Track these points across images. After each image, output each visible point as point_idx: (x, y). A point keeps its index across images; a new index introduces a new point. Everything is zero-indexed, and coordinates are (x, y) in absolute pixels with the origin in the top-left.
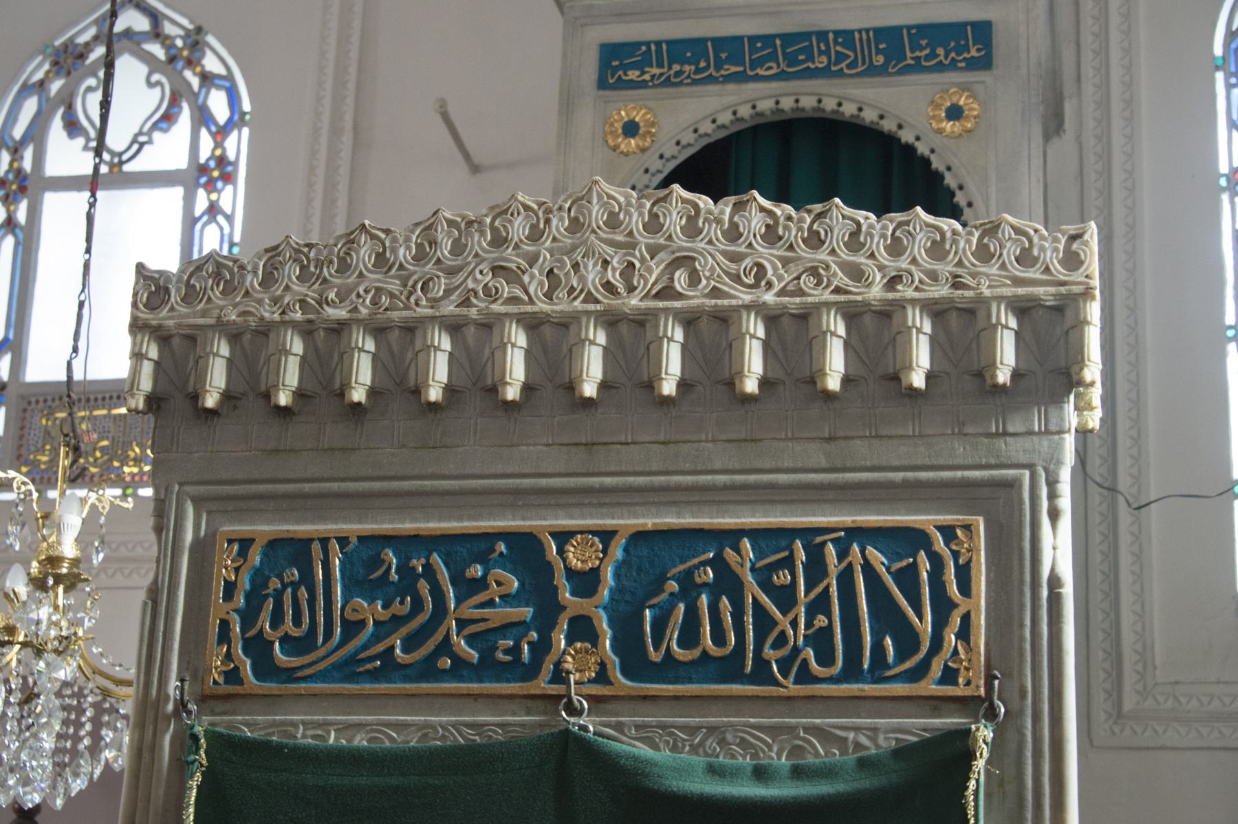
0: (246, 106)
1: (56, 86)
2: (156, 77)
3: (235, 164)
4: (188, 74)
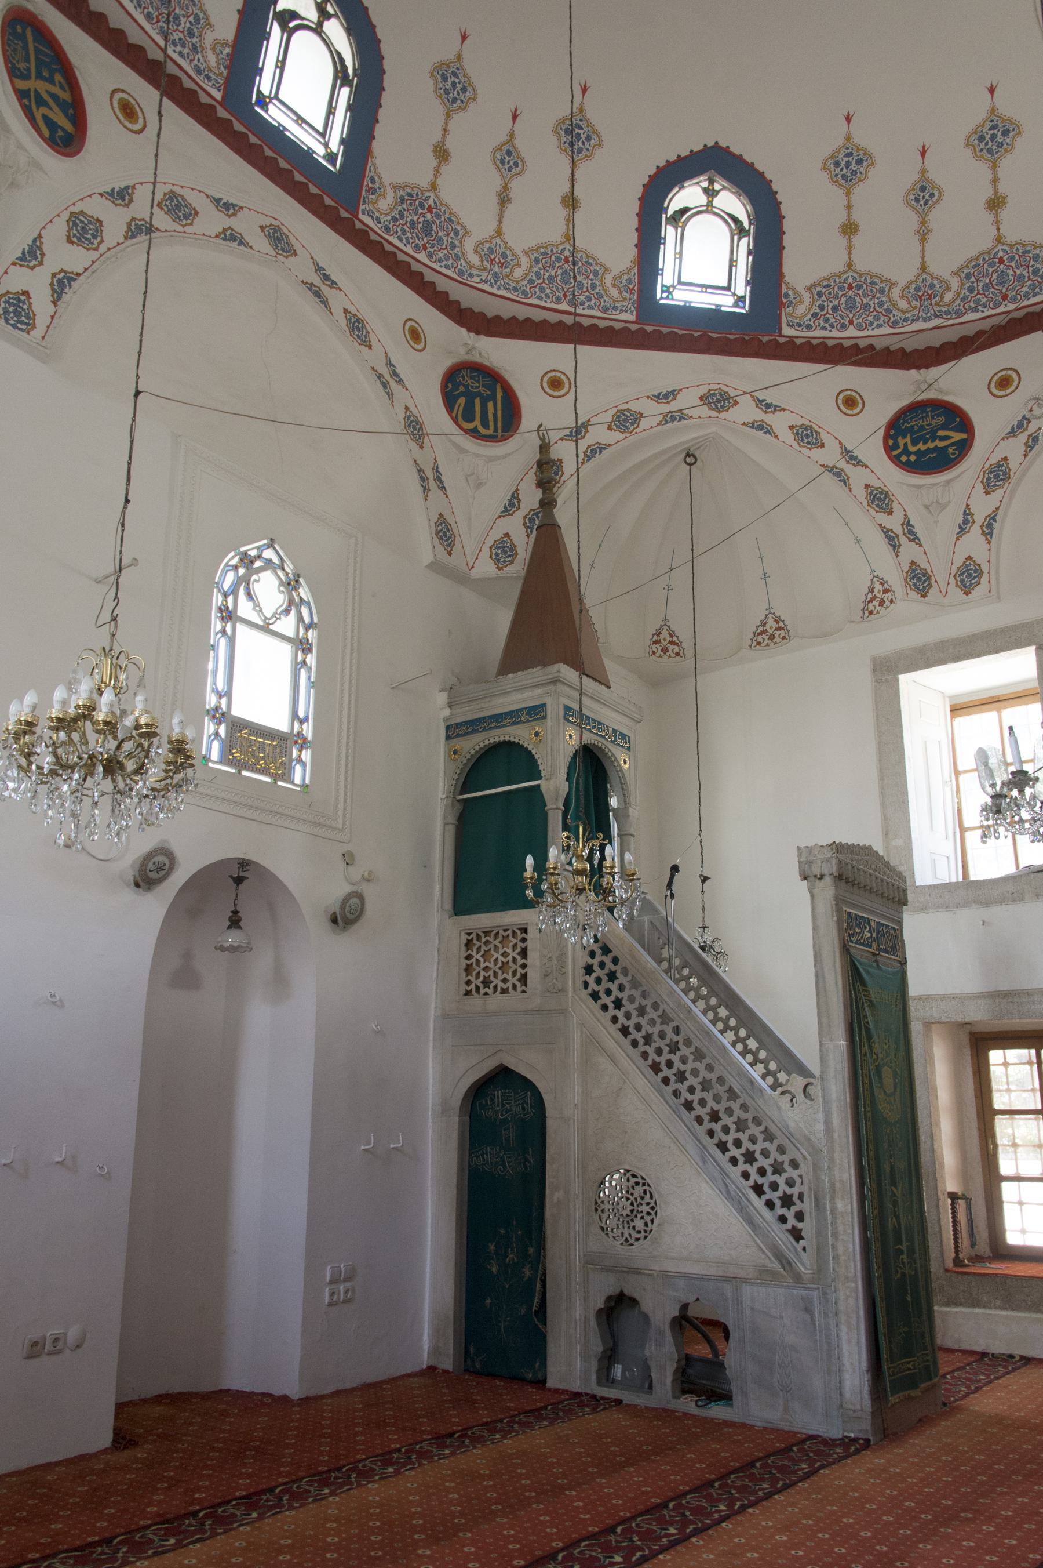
0: (315, 620)
1: (242, 571)
2: (282, 589)
3: (311, 644)
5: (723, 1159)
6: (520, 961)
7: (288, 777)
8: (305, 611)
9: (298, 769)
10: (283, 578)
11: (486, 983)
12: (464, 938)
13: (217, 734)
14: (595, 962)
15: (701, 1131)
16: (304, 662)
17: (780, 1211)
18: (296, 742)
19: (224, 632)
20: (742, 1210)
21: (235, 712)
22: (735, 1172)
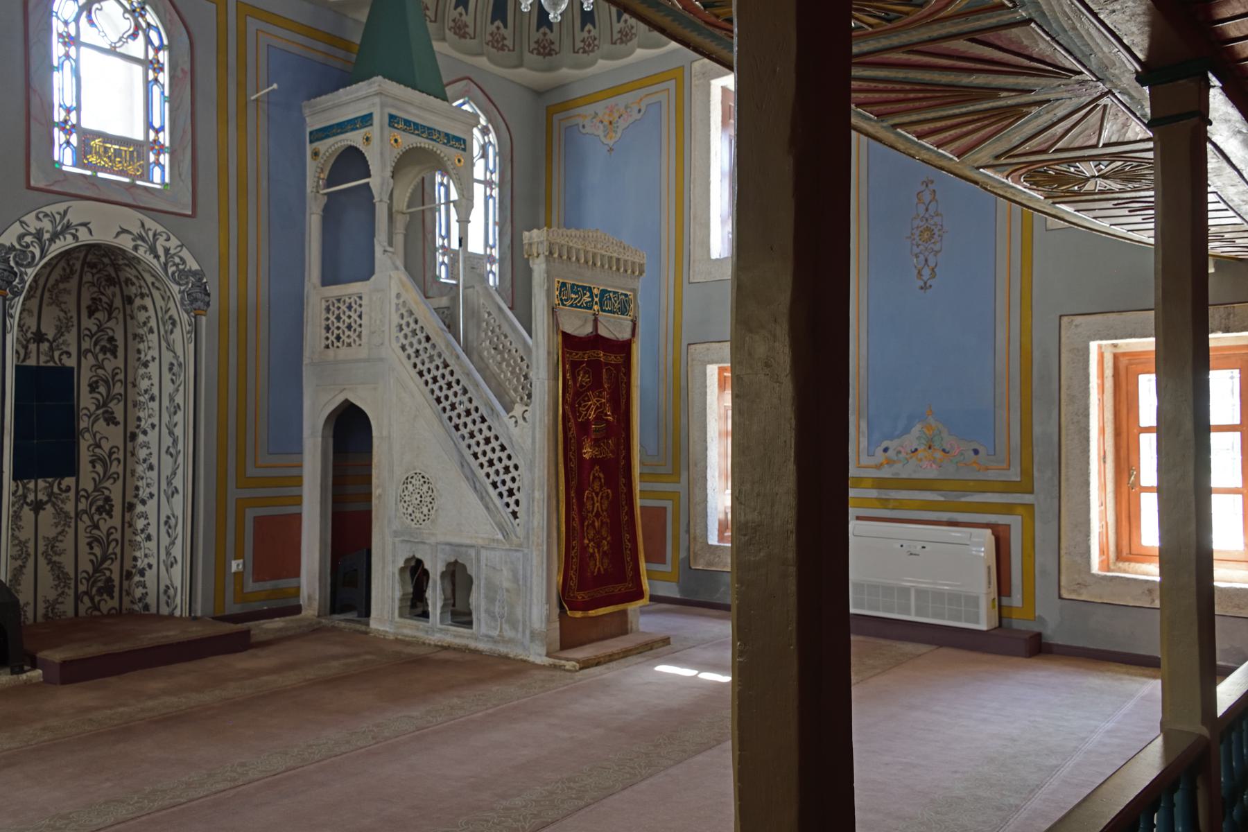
2: (127, 15)
4: (140, 19)
5: (474, 464)
6: (359, 321)
7: (147, 176)
8: (153, 35)
9: (157, 172)
10: (128, 6)
11: (338, 338)
12: (324, 305)
13: (68, 143)
14: (404, 322)
15: (463, 444)
16: (156, 80)
17: (506, 499)
18: (152, 149)
19: (67, 56)
20: (482, 499)
21: (87, 124)
22: (481, 473)
